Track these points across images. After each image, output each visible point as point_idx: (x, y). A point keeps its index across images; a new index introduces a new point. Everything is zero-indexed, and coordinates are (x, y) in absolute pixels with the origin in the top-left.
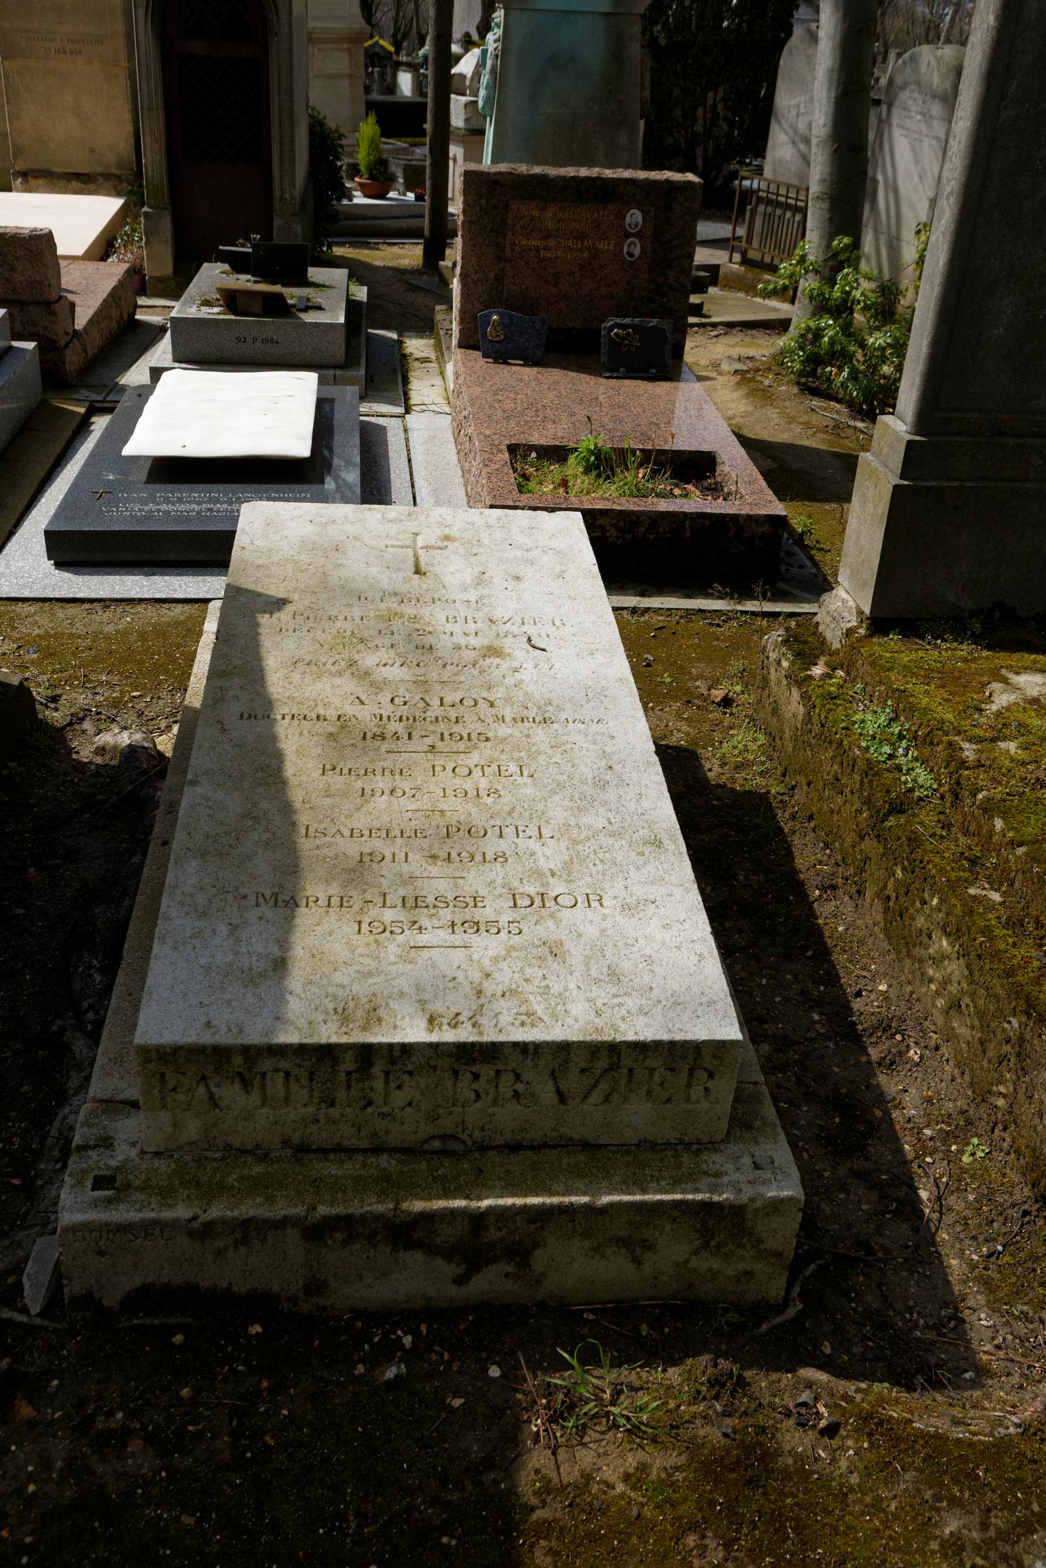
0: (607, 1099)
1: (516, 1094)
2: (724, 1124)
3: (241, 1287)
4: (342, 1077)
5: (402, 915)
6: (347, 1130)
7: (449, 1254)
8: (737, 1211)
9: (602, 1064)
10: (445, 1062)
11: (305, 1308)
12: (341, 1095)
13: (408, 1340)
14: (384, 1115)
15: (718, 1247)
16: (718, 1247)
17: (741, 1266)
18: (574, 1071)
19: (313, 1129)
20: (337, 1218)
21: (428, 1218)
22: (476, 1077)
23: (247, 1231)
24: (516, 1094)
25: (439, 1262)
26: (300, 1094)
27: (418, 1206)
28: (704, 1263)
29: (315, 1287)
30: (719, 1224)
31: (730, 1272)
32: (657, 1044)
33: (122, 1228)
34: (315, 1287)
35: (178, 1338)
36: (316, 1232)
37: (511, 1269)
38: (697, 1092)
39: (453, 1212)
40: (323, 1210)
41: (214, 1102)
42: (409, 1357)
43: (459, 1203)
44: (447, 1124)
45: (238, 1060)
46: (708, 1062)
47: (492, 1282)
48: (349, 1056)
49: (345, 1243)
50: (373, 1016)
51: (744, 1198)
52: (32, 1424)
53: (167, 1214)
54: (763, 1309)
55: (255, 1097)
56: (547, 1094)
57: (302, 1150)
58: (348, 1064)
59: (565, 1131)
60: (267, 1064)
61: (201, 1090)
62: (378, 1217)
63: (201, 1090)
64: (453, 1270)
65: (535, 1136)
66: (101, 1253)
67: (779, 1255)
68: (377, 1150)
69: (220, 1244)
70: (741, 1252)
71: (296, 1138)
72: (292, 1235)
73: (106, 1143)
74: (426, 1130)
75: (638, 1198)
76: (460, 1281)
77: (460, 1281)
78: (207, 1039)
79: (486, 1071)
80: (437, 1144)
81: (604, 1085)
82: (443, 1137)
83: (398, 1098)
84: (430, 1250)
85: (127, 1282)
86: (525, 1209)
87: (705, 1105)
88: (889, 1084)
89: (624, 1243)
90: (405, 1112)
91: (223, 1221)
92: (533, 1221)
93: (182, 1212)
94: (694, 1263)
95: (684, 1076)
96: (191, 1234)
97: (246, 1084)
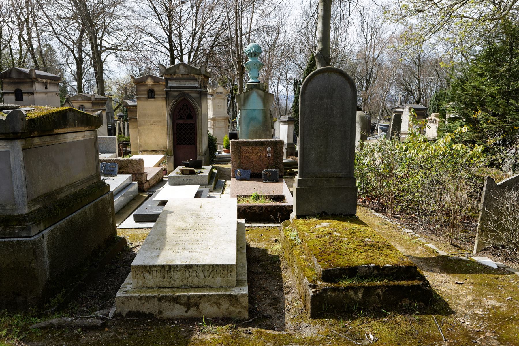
0: (213, 277)
1: (197, 276)
2: (235, 283)
3: (147, 312)
4: (166, 272)
5: (181, 250)
6: (167, 284)
7: (184, 305)
8: (236, 296)
9: (211, 269)
10: (183, 269)
11: (158, 317)
12: (166, 276)
13: (176, 322)
14: (174, 280)
15: (234, 305)
16: (234, 305)
17: (239, 310)
18: (206, 270)
19: (161, 283)
20: (164, 296)
21: (180, 296)
22: (189, 272)
23: (148, 298)
24: (197, 276)
25: (182, 307)
26: (159, 275)
27: (178, 294)
28: (232, 309)
29: (160, 312)
30: (233, 299)
31: (237, 311)
32: (220, 265)
33: (127, 298)
34: (160, 312)
35: (135, 321)
36: (160, 299)
37: (195, 309)
38: (229, 275)
39: (184, 295)
40: (161, 294)
41: (144, 277)
42: (176, 324)
43: (185, 294)
44: (185, 282)
45: (148, 268)
46: (230, 269)
47: (192, 312)
48: (167, 267)
49: (165, 302)
50: (172, 261)
51: (237, 294)
52: (108, 331)
53: (134, 295)
54: (244, 320)
55: (151, 276)
56: (202, 276)
57: (160, 288)
58: (167, 269)
59: (206, 284)
60: (153, 269)
61: (142, 274)
62: (171, 296)
63: (142, 274)
64: (185, 309)
65: (201, 285)
66: (123, 303)
67: (245, 307)
68: (173, 288)
69: (143, 301)
70: (238, 306)
71: (158, 285)
72: (156, 300)
73: (126, 287)
74: (181, 283)
75: (217, 293)
76: (187, 312)
77: (187, 312)
78: (143, 264)
79: (191, 270)
80: (183, 287)
81: (212, 274)
82: (184, 285)
83: (176, 276)
84: (181, 304)
85: (127, 310)
86: (197, 295)
87: (231, 278)
88: (286, 296)
89: (216, 303)
90: (177, 278)
91: (144, 296)
92: (198, 298)
93: (137, 295)
94: (229, 309)
95: (226, 271)
96: (138, 299)
97: (150, 273)
